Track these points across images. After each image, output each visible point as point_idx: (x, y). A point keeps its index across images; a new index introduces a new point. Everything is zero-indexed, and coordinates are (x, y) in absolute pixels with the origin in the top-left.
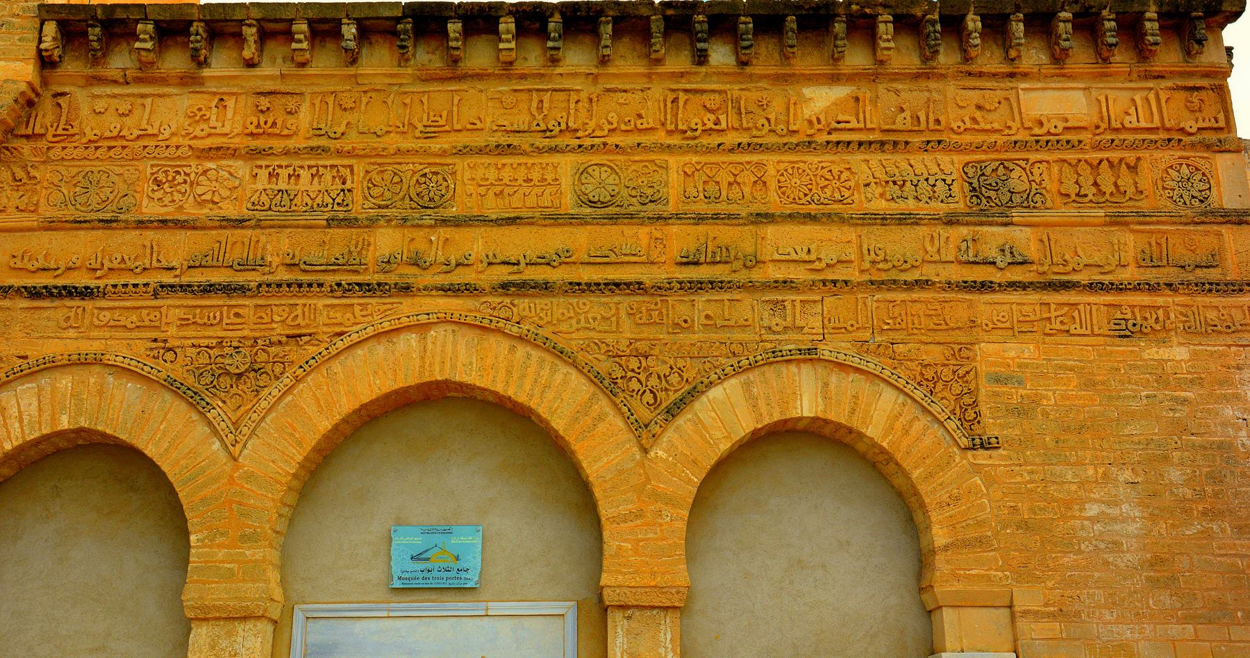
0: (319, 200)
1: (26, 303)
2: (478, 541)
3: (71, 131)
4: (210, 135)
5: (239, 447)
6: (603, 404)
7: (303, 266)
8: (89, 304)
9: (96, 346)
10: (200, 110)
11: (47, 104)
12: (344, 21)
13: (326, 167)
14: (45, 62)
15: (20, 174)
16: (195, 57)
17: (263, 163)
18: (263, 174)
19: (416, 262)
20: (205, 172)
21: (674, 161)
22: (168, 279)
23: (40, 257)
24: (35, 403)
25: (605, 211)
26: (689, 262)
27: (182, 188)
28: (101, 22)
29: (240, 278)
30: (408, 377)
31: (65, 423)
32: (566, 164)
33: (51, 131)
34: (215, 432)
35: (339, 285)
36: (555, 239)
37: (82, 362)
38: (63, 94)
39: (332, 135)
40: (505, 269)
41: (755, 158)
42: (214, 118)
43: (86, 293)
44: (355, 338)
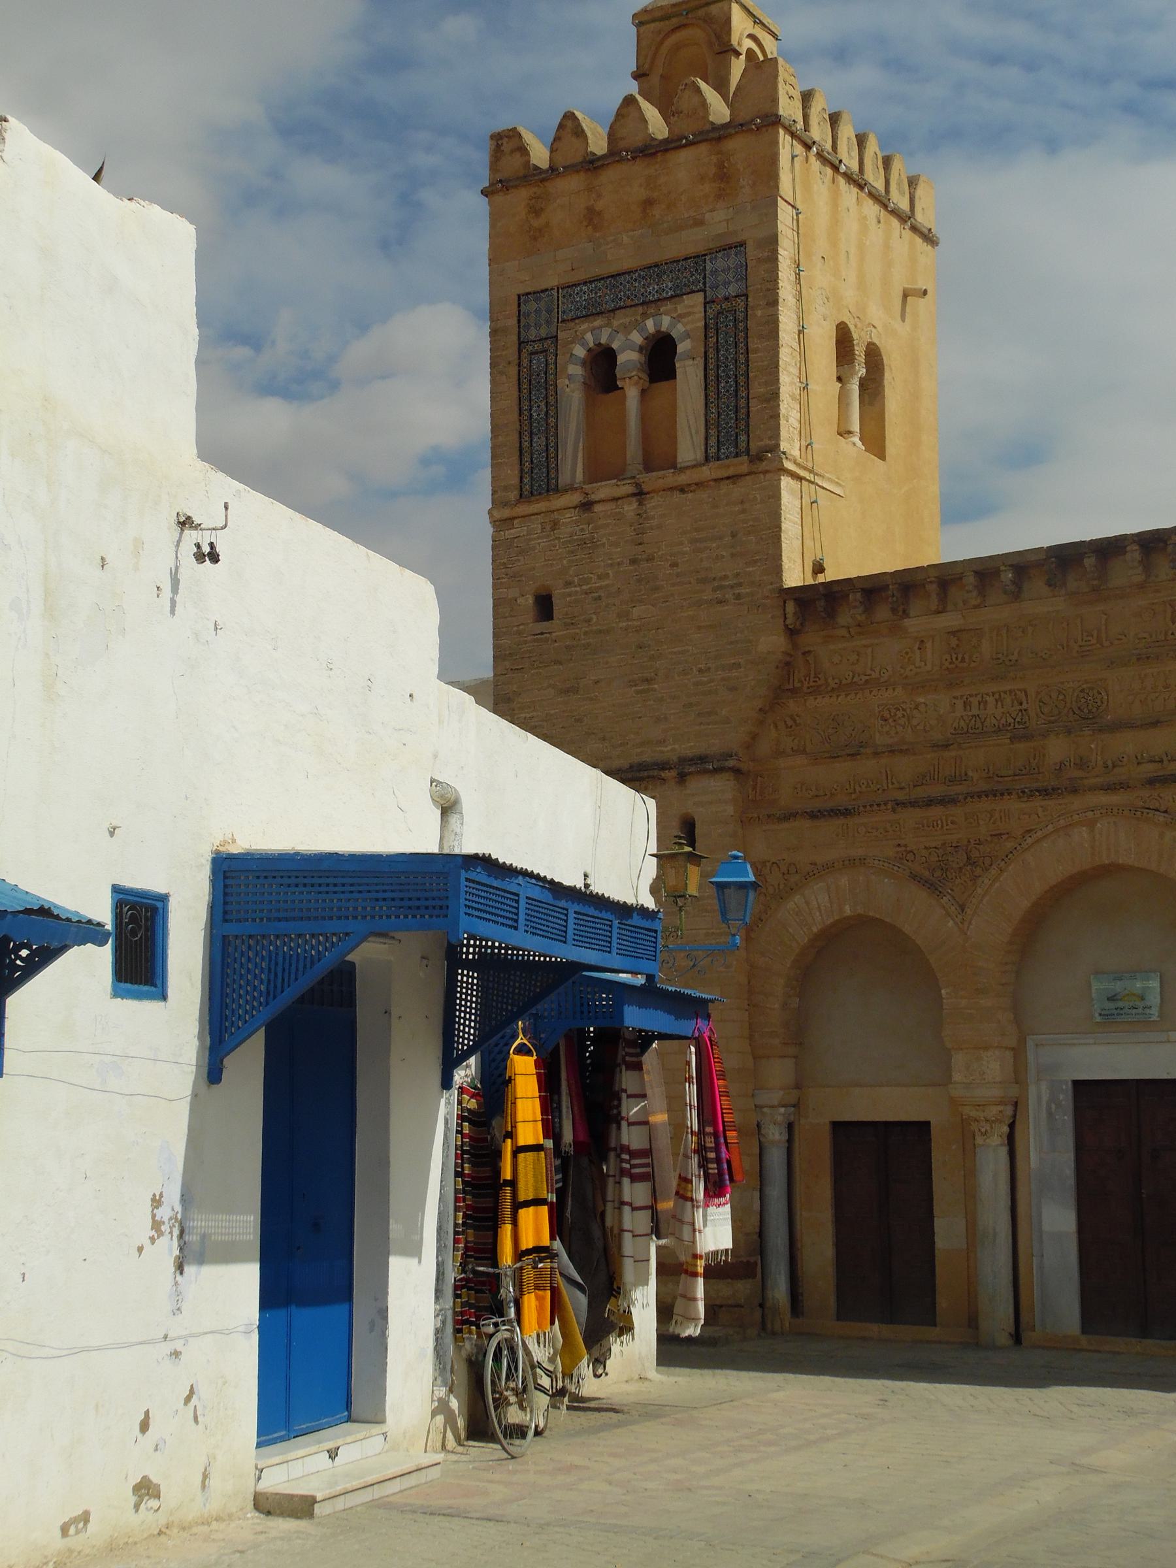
0: (1003, 721)
2: (1155, 984)
3: (819, 683)
4: (917, 674)
5: (966, 924)
7: (996, 779)
10: (907, 653)
12: (1003, 568)
13: (1005, 692)
14: (792, 633)
15: (790, 723)
17: (958, 694)
18: (959, 704)
19: (1082, 764)
20: (916, 708)
22: (901, 796)
23: (814, 788)
24: (827, 898)
27: (902, 721)
28: (825, 595)
31: (848, 911)
33: (806, 685)
34: (948, 914)
35: (1023, 792)
37: (852, 863)
38: (809, 652)
39: (1008, 663)
40: (1151, 766)
42: (918, 659)
43: (847, 813)
44: (1039, 834)
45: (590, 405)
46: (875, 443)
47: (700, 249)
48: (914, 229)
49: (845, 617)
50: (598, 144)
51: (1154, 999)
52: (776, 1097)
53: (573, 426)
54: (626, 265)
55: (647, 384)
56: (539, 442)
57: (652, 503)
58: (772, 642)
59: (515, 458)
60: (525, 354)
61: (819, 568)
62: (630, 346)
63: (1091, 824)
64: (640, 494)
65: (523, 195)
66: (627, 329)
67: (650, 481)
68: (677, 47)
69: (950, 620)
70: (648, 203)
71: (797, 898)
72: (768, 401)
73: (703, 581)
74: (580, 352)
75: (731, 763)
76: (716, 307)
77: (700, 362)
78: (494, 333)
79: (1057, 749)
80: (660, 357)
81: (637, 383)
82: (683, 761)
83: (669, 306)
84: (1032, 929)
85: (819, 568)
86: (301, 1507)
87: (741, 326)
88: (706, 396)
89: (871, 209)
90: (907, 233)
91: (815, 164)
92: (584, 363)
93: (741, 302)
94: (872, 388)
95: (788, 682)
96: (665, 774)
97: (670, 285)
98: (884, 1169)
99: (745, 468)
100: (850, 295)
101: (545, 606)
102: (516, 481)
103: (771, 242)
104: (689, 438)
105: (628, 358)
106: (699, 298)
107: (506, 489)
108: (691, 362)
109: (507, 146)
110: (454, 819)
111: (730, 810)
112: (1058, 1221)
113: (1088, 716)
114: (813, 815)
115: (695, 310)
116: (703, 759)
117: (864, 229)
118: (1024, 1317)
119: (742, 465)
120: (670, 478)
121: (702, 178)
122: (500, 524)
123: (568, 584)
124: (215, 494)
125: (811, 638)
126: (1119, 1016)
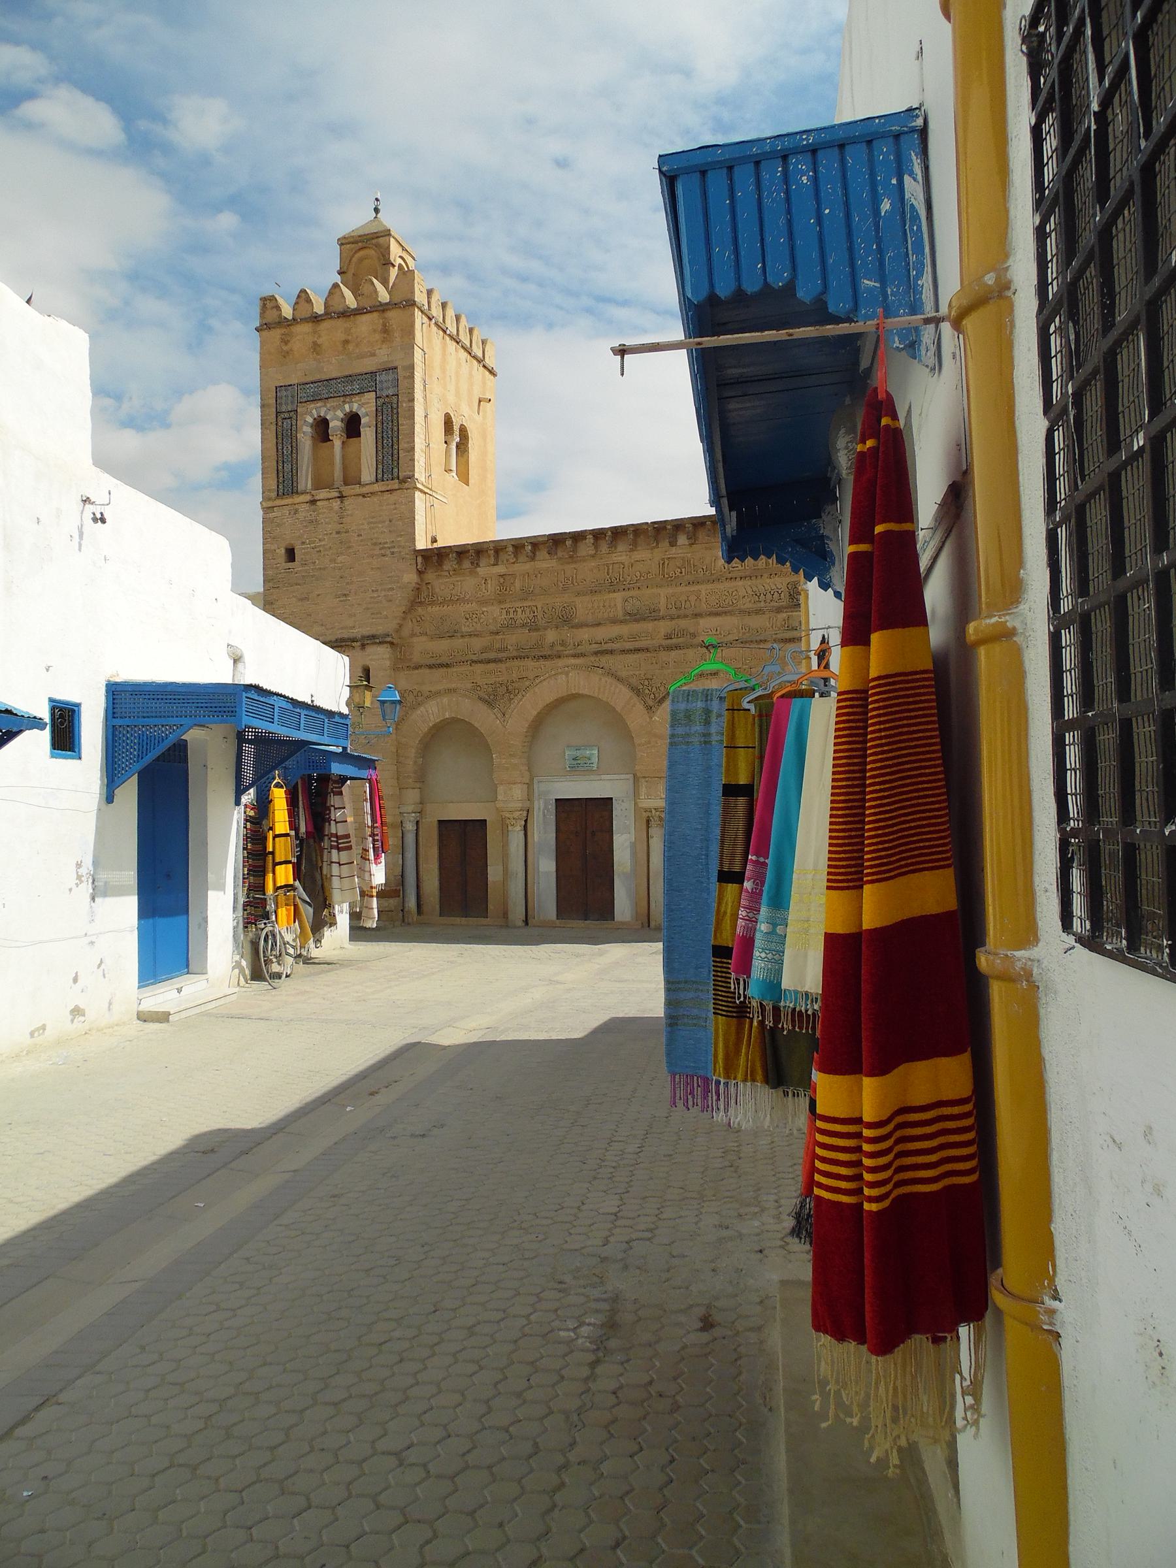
1: (428, 671)
6: (635, 698)
8: (449, 670)
9: (454, 686)
11: (424, 587)
14: (420, 573)
16: (472, 563)
19: (563, 643)
21: (664, 592)
22: (474, 658)
25: (634, 617)
26: (668, 637)
29: (501, 655)
30: (563, 692)
32: (618, 597)
36: (615, 630)
41: (696, 588)
43: (447, 666)
45: (315, 447)
46: (464, 477)
47: (374, 369)
48: (484, 366)
49: (448, 565)
50: (319, 308)
51: (595, 760)
52: (410, 808)
53: (306, 459)
54: (334, 376)
56: (288, 467)
57: (347, 502)
58: (411, 577)
61: (434, 540)
63: (567, 674)
64: (341, 497)
65: (276, 334)
66: (335, 408)
67: (347, 490)
68: (361, 260)
69: (500, 569)
70: (346, 342)
71: (422, 709)
73: (375, 544)
74: (310, 420)
75: (389, 639)
78: (262, 406)
79: (551, 636)
80: (353, 425)
82: (363, 637)
84: (537, 726)
85: (434, 540)
86: (164, 1017)
89: (463, 355)
90: (481, 368)
91: (434, 328)
94: (462, 447)
95: (418, 598)
96: (354, 644)
98: (464, 844)
99: (396, 486)
100: (451, 399)
101: (291, 554)
103: (412, 367)
105: (336, 425)
107: (269, 490)
109: (269, 305)
110: (240, 665)
111: (388, 663)
112: (546, 866)
113: (566, 620)
114: (430, 667)
116: (374, 637)
117: (459, 365)
118: (530, 913)
119: (395, 484)
120: (357, 489)
121: (375, 331)
122: (267, 510)
123: (303, 543)
124: (102, 485)
125: (430, 576)
126: (578, 767)
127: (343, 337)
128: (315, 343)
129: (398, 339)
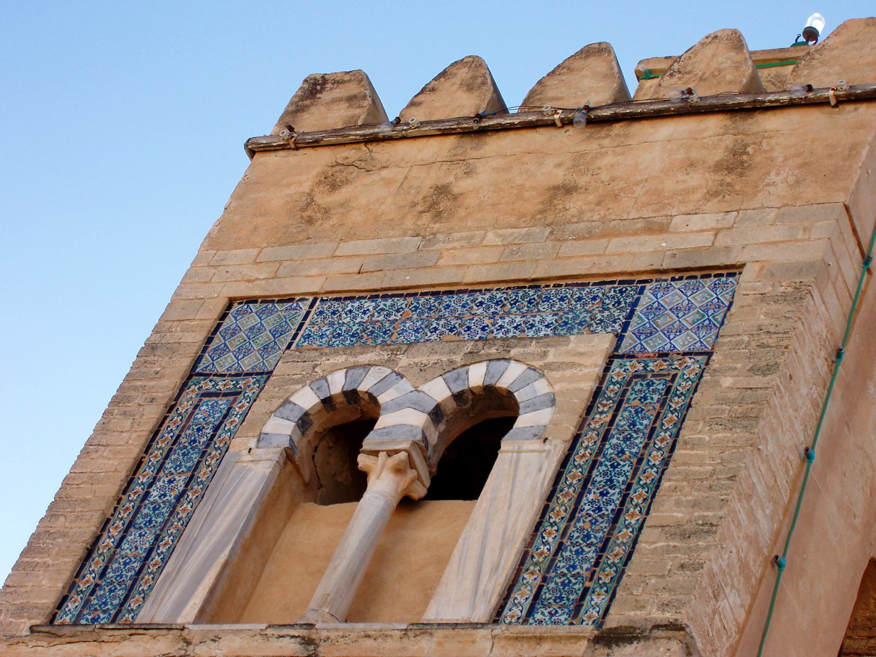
47: (642, 265)
54: (471, 276)
55: (420, 491)
56: (138, 542)
59: (69, 563)
60: (192, 393)
62: (416, 406)
66: (424, 372)
72: (685, 536)
74: (307, 399)
76: (633, 366)
77: (557, 449)
78: (151, 348)
81: (398, 470)
83: (533, 348)
87: (676, 403)
88: (545, 510)
92: (304, 422)
93: (693, 365)
97: (549, 319)
102: (49, 600)
104: (468, 584)
106: (603, 342)
108: (537, 445)
115: (588, 361)
121: (691, 165)
127: (559, 176)
128: (442, 190)
129: (781, 189)
